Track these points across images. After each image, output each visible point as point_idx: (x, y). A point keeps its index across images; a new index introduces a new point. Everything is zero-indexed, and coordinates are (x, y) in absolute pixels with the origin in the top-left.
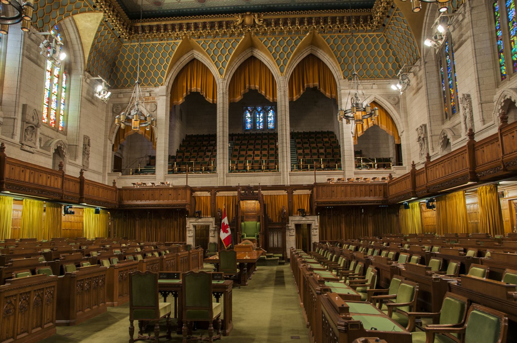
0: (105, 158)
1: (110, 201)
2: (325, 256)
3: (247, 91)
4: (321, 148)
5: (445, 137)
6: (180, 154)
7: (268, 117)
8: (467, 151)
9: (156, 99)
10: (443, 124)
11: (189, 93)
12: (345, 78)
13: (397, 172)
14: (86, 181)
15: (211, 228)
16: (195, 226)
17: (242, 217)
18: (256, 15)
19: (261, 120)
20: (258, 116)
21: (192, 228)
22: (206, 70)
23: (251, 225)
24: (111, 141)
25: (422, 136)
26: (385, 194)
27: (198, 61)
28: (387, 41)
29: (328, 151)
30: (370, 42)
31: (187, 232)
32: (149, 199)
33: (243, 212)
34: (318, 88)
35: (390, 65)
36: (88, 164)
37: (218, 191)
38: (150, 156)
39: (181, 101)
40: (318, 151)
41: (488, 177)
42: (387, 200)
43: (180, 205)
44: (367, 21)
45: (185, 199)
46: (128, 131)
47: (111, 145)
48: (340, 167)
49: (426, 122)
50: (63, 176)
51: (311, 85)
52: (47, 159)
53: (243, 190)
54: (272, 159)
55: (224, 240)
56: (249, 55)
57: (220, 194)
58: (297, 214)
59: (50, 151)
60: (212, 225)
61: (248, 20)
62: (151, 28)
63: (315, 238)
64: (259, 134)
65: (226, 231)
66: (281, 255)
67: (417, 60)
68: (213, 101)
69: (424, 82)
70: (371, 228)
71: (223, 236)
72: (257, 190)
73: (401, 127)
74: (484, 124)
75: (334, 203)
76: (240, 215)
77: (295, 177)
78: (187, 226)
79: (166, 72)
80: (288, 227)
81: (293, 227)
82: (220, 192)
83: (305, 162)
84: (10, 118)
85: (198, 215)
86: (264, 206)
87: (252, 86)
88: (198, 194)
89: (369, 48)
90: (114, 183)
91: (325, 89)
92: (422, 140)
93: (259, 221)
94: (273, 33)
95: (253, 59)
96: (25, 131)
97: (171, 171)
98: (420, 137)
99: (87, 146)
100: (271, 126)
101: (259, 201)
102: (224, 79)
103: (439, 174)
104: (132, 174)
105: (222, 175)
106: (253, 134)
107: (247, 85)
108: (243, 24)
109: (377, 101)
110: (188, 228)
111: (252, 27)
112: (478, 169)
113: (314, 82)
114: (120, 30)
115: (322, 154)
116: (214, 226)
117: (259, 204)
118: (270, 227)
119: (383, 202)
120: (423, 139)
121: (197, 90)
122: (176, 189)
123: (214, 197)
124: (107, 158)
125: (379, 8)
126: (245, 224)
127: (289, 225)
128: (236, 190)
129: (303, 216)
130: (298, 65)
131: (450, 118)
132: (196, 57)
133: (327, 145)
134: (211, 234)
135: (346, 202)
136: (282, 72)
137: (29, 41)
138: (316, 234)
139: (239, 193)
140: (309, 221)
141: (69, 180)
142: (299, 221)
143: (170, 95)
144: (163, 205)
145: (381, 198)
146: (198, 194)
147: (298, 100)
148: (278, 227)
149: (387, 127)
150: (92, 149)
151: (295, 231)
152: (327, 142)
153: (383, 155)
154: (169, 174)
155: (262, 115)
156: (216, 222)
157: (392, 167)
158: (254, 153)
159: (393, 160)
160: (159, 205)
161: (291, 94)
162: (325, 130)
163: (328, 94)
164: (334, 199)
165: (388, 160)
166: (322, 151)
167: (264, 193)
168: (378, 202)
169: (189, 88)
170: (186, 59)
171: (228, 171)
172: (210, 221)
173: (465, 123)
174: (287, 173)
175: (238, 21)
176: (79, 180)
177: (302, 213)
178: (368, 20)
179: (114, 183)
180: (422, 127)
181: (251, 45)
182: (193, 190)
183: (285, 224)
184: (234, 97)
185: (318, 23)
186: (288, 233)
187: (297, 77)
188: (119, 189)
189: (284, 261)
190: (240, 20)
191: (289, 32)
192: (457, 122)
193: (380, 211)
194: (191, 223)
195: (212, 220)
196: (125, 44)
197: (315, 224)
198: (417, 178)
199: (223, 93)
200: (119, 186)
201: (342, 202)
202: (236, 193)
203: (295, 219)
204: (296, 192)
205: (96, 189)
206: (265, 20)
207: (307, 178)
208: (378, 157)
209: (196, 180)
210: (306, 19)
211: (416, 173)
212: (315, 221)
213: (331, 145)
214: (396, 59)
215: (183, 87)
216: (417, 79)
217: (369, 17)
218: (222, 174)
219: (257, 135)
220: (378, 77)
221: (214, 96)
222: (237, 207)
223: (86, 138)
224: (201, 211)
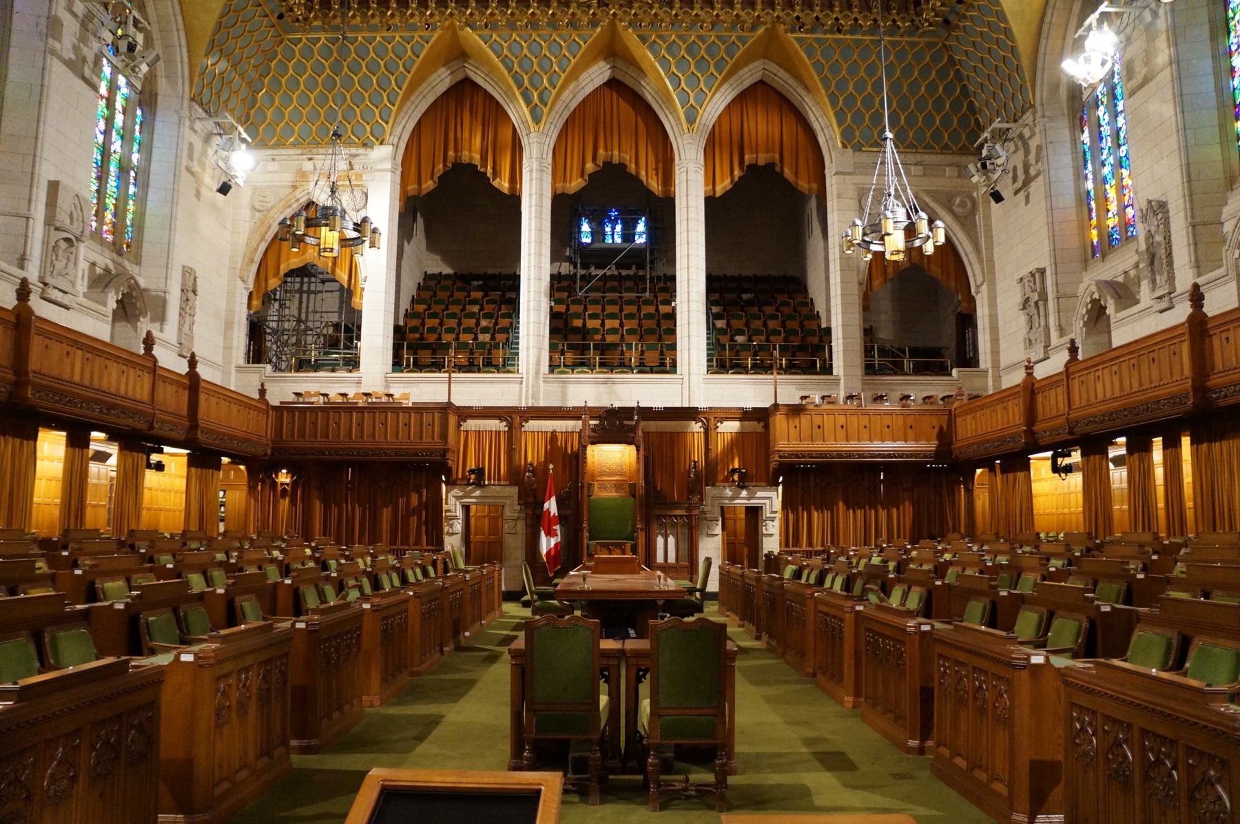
0: (229, 325)
1: (254, 438)
4: (773, 317)
6: (414, 322)
7: (634, 235)
8: (1186, 337)
9: (364, 177)
11: (450, 165)
12: (845, 146)
14: (203, 384)
15: (508, 513)
20: (608, 229)
22: (494, 113)
25: (1035, 297)
29: (792, 324)
34: (778, 169)
39: (429, 185)
42: (950, 452)
44: (907, 9)
46: (288, 259)
49: (1045, 262)
50: (155, 371)
52: (99, 324)
53: (592, 418)
54: (652, 340)
57: (533, 425)
59: (105, 305)
67: (1023, 113)
75: (822, 455)
79: (394, 109)
82: (531, 422)
90: (262, 392)
92: (1034, 305)
96: (51, 250)
97: (397, 364)
98: (1027, 300)
99: (190, 295)
105: (530, 377)
110: (449, 511)
112: (1214, 381)
116: (518, 508)
118: (657, 512)
120: (1036, 303)
124: (236, 326)
128: (579, 418)
131: (1104, 257)
133: (787, 310)
141: (165, 380)
143: (400, 169)
147: (727, 194)
148: (678, 512)
149: (942, 273)
154: (394, 371)
155: (619, 228)
157: (955, 372)
161: (711, 179)
165: (936, 352)
169: (451, 153)
171: (547, 369)
176: (186, 381)
179: (262, 392)
180: (1033, 275)
184: (564, 181)
188: (274, 408)
197: (771, 506)
200: (274, 399)
201: (840, 455)
205: (224, 405)
209: (472, 390)
211: (1036, 386)
221: (515, 177)
222: (576, 461)
224: (483, 469)
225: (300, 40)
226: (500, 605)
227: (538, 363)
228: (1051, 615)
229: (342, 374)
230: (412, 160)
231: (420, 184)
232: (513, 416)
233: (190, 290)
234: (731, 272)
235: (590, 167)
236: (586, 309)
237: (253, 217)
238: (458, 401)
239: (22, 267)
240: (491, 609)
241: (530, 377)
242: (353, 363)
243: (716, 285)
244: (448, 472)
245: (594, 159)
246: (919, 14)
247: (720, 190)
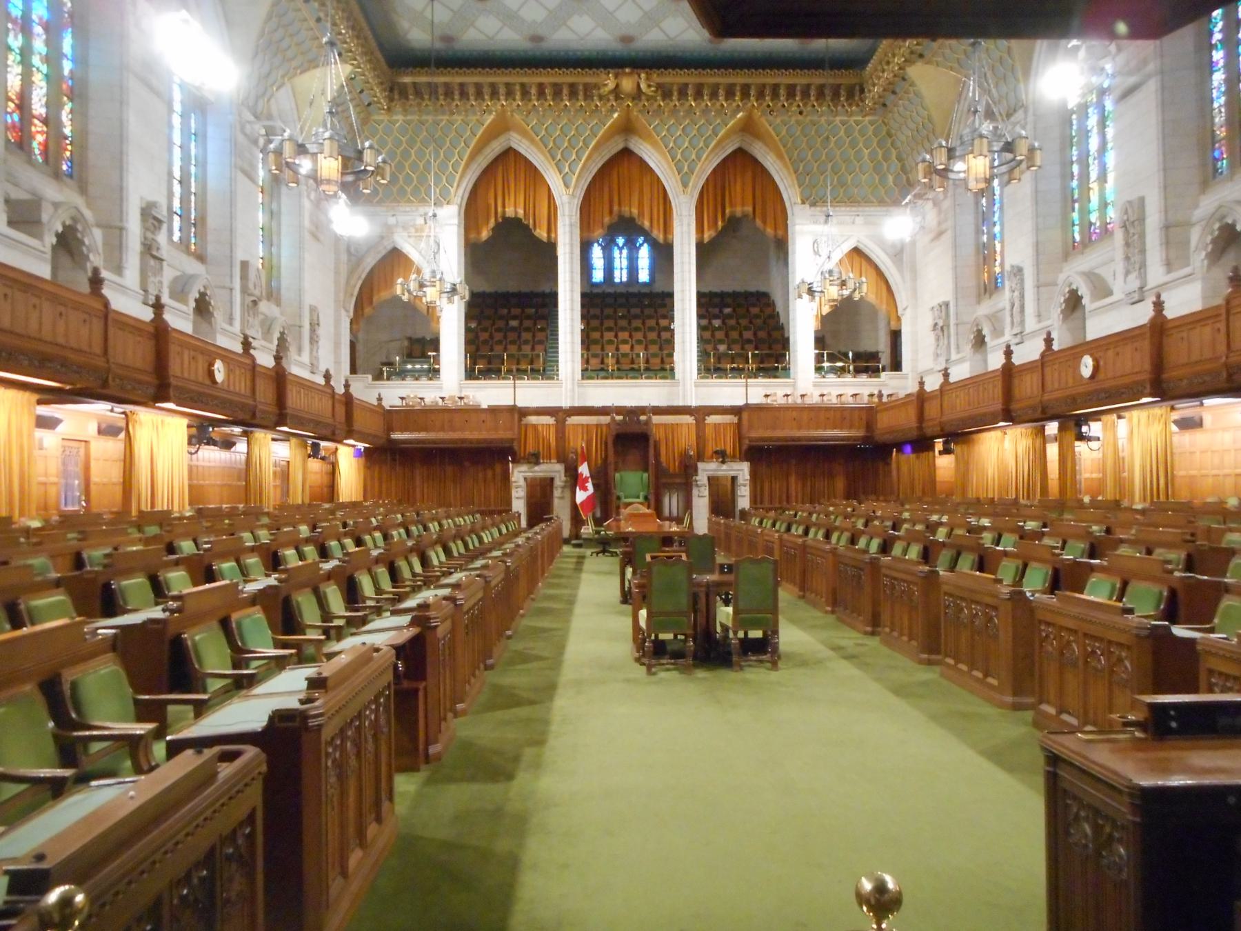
3: (615, 219)
4: (747, 328)
5: (979, 332)
10: (979, 302)
12: (803, 203)
13: (894, 385)
16: (525, 479)
18: (643, 75)
19: (625, 263)
21: (522, 483)
22: (533, 175)
24: (347, 311)
25: (941, 323)
26: (869, 426)
27: (517, 154)
28: (889, 134)
29: (762, 334)
30: (856, 134)
32: (442, 429)
35: (890, 178)
36: (317, 358)
37: (569, 416)
38: (410, 339)
39: (485, 234)
40: (741, 335)
41: (1026, 418)
43: (502, 440)
45: (511, 429)
46: (379, 291)
47: (348, 321)
48: (786, 370)
49: (947, 295)
51: (739, 211)
53: (618, 414)
54: (654, 349)
55: (582, 503)
56: (621, 146)
59: (271, 342)
61: (627, 84)
62: (433, 89)
63: (744, 502)
64: (621, 295)
65: (585, 489)
68: (549, 236)
69: (950, 223)
70: (840, 484)
71: (581, 496)
72: (644, 414)
73: (902, 298)
74: (1040, 322)
75: (778, 439)
77: (705, 389)
79: (458, 176)
81: (705, 481)
83: (719, 358)
84: (224, 287)
85: (535, 459)
87: (626, 210)
88: (533, 419)
89: (853, 145)
90: (380, 399)
91: (764, 222)
92: (940, 329)
93: (646, 470)
94: (674, 111)
95: (626, 153)
97: (470, 374)
100: (644, 276)
102: (573, 196)
103: (958, 407)
104: (388, 379)
105: (569, 384)
106: (609, 295)
107: (616, 208)
108: (617, 91)
109: (861, 247)
111: (634, 99)
113: (743, 205)
114: (379, 94)
115: (749, 341)
116: (563, 478)
118: (664, 480)
119: (866, 440)
120: (942, 328)
121: (516, 213)
122: (493, 410)
123: (561, 428)
125: (879, 78)
128: (607, 414)
129: (723, 462)
130: (714, 171)
131: (991, 296)
132: (515, 146)
133: (759, 322)
134: (557, 493)
135: (799, 439)
136: (685, 185)
137: (241, 138)
139: (613, 419)
144: (471, 441)
145: (860, 433)
146: (533, 419)
147: (713, 242)
150: (321, 331)
152: (757, 316)
153: (867, 346)
158: (616, 336)
159: (885, 359)
160: (463, 441)
162: (752, 289)
163: (770, 231)
164: (779, 433)
165: (874, 356)
166: (748, 335)
167: (656, 419)
168: (856, 438)
169: (500, 210)
170: (496, 148)
173: (1012, 315)
174: (689, 385)
175: (606, 85)
177: (722, 456)
178: (855, 93)
179: (380, 399)
181: (627, 128)
182: (524, 412)
185: (760, 95)
186: (695, 492)
187: (713, 196)
190: (611, 84)
191: (706, 111)
192: (1001, 305)
193: (858, 458)
194: (519, 475)
196: (376, 117)
198: (927, 405)
199: (571, 225)
201: (793, 439)
202: (605, 420)
203: (706, 469)
204: (712, 419)
206: (659, 86)
207: (731, 392)
208: (856, 350)
209: (528, 393)
210: (738, 88)
212: (742, 470)
213: (764, 322)
214: (903, 169)
215: (488, 206)
216: (940, 212)
217: (857, 88)
218: (569, 382)
219: (616, 296)
220: (866, 201)
223: (313, 309)
225: (382, 121)
227: (573, 373)
228: (959, 554)
229: (424, 381)
230: (472, 214)
231: (479, 233)
232: (559, 414)
233: (314, 326)
234: (716, 289)
235: (607, 220)
236: (602, 324)
237: (349, 260)
238: (520, 404)
239: (231, 324)
241: (569, 384)
242: (434, 373)
243: (703, 300)
244: (514, 454)
245: (611, 212)
246: (862, 100)
247: (708, 235)
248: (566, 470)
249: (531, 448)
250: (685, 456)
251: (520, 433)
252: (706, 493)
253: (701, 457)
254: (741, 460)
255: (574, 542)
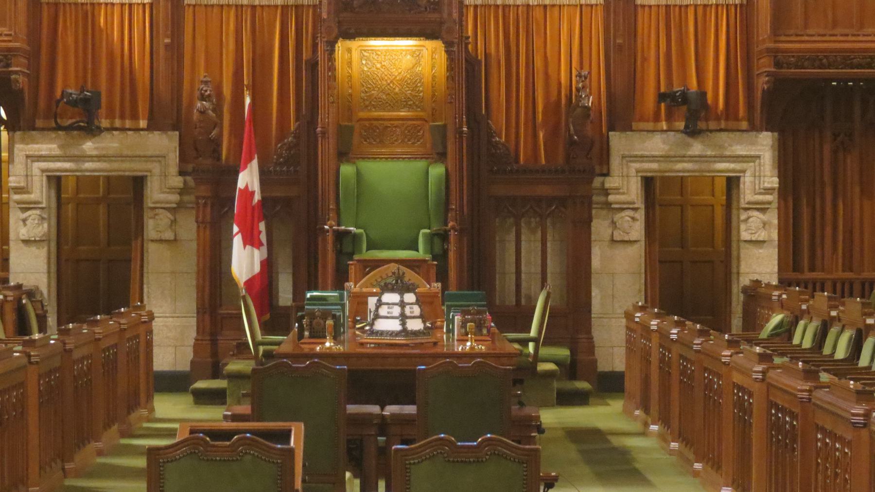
2: (827, 351)
15: (156, 193)
16: (56, 181)
17: (344, 133)
21: (39, 192)
23: (396, 178)
31: (15, 217)
33: (348, 107)
58: (657, 118)
60: (164, 175)
66: (563, 353)
76: (327, 118)
78: (13, 181)
80: (606, 192)
81: (634, 192)
85: (82, 116)
86: (467, 71)
93: (441, 157)
101: (448, 45)
110: (19, 190)
116: (177, 181)
117: (441, 57)
126: (358, 173)
127: (611, 182)
129: (692, 132)
134: (155, 226)
138: (762, 235)
140: (723, 158)
142: (666, 158)
148: (543, 190)
151: (641, 215)
156: (183, 158)
172: (154, 154)
183: (592, 174)
186: (600, 227)
189: (583, 385)
195: (165, 144)
203: (642, 152)
212: (754, 161)
222: (312, 73)
224: (98, 94)
226: (149, 398)
240: (133, 403)
248: (188, 153)
249: (67, 84)
250: (566, 111)
251: (34, 33)
252: (637, 231)
253: (622, 114)
254: (753, 128)
255: (201, 384)
